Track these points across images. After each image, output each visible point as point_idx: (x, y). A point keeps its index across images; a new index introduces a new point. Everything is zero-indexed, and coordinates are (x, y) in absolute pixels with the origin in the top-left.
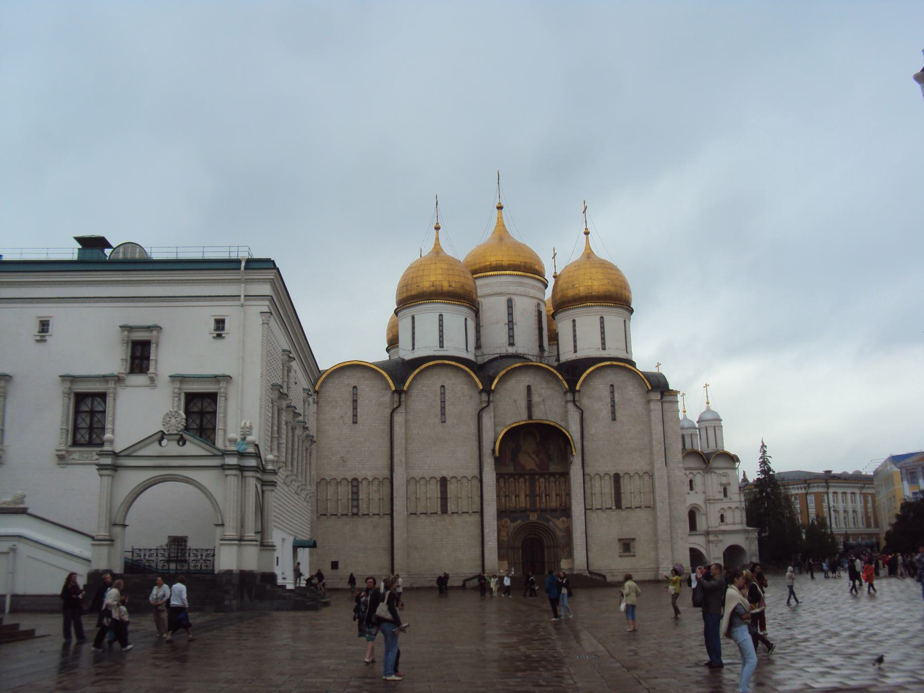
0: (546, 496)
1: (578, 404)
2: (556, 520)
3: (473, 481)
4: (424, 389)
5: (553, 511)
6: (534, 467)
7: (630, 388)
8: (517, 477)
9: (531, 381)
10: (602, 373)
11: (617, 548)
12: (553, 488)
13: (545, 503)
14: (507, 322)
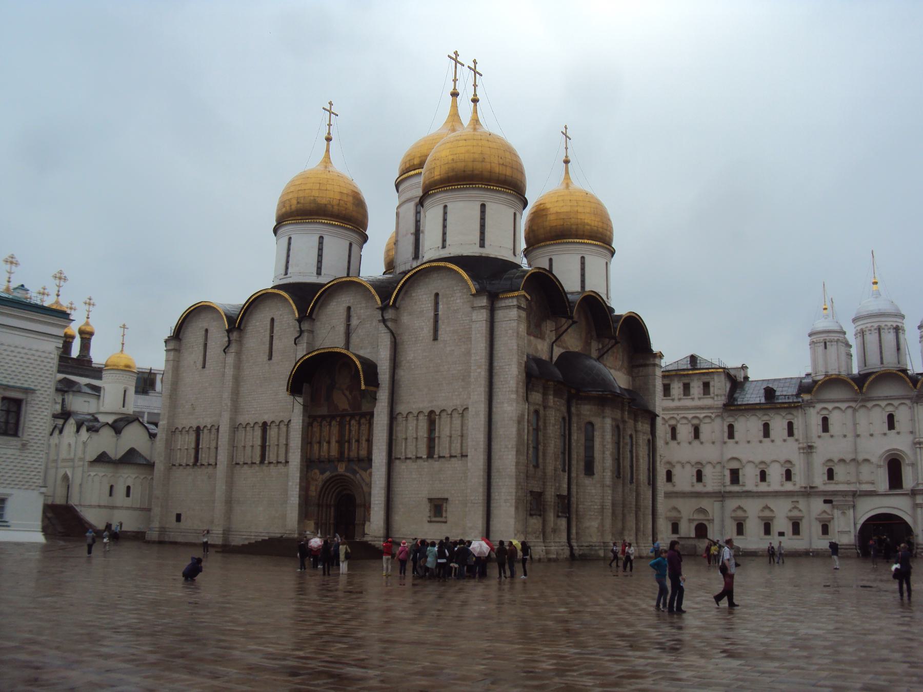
1: (389, 324)
4: (257, 324)
5: (360, 460)
6: (347, 407)
7: (457, 295)
8: (328, 420)
9: (352, 301)
10: (427, 280)
11: (426, 509)
12: (364, 432)
14: (413, 230)
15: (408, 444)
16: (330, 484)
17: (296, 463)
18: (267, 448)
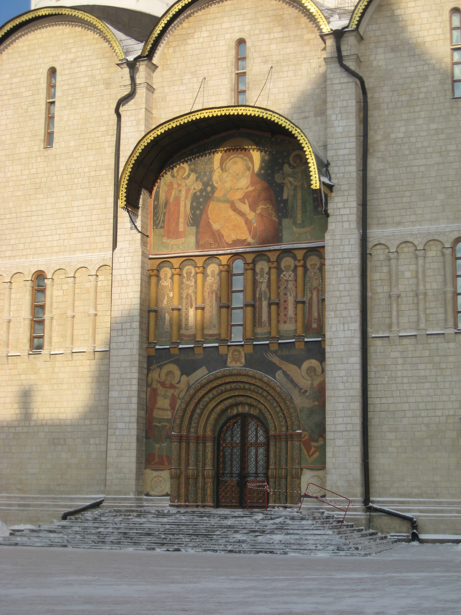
0: (270, 305)
1: (351, 65)
2: (291, 366)
3: (100, 278)
9: (247, 28)
13: (267, 324)
15: (403, 307)
16: (203, 396)
17: (127, 352)
18: (47, 323)
